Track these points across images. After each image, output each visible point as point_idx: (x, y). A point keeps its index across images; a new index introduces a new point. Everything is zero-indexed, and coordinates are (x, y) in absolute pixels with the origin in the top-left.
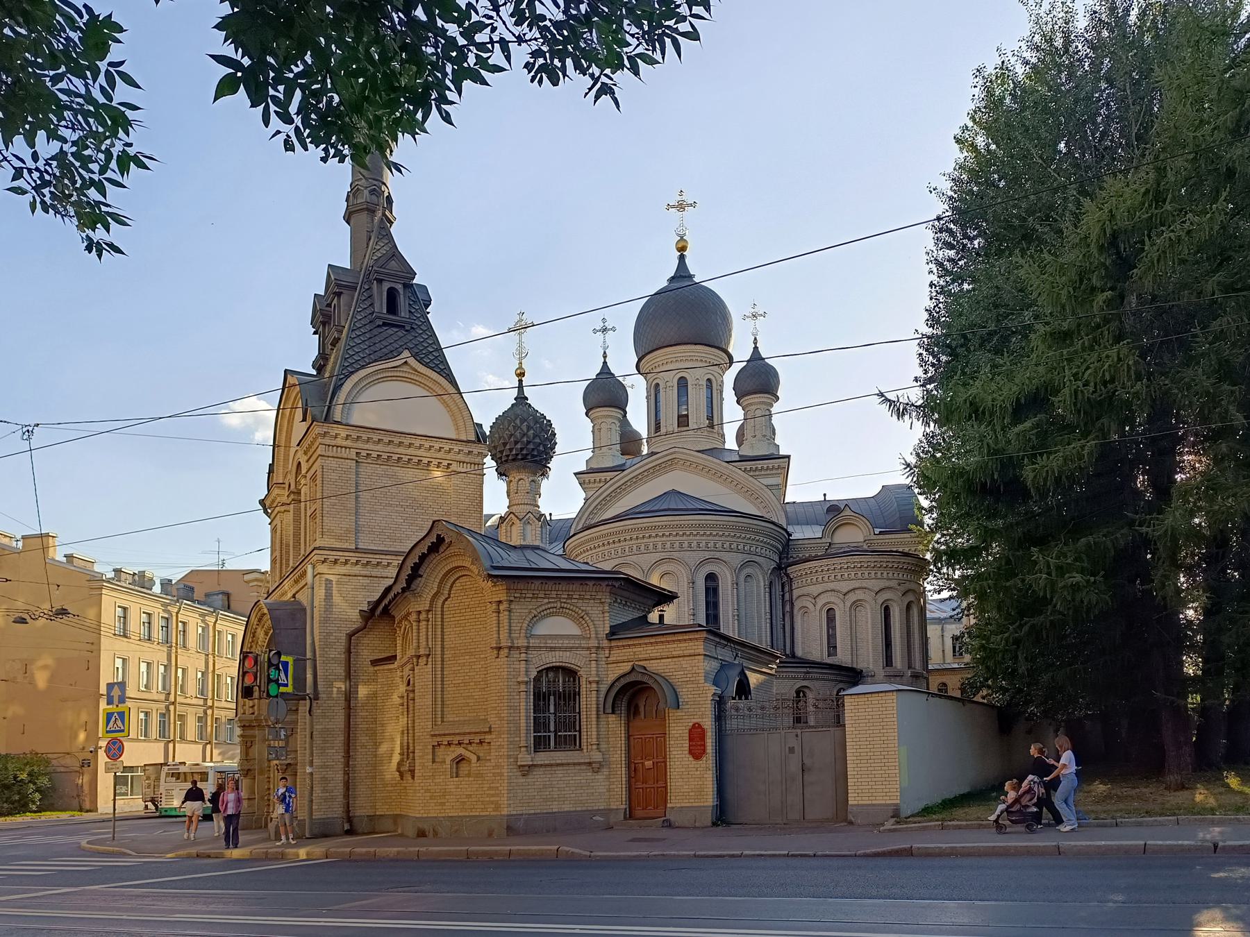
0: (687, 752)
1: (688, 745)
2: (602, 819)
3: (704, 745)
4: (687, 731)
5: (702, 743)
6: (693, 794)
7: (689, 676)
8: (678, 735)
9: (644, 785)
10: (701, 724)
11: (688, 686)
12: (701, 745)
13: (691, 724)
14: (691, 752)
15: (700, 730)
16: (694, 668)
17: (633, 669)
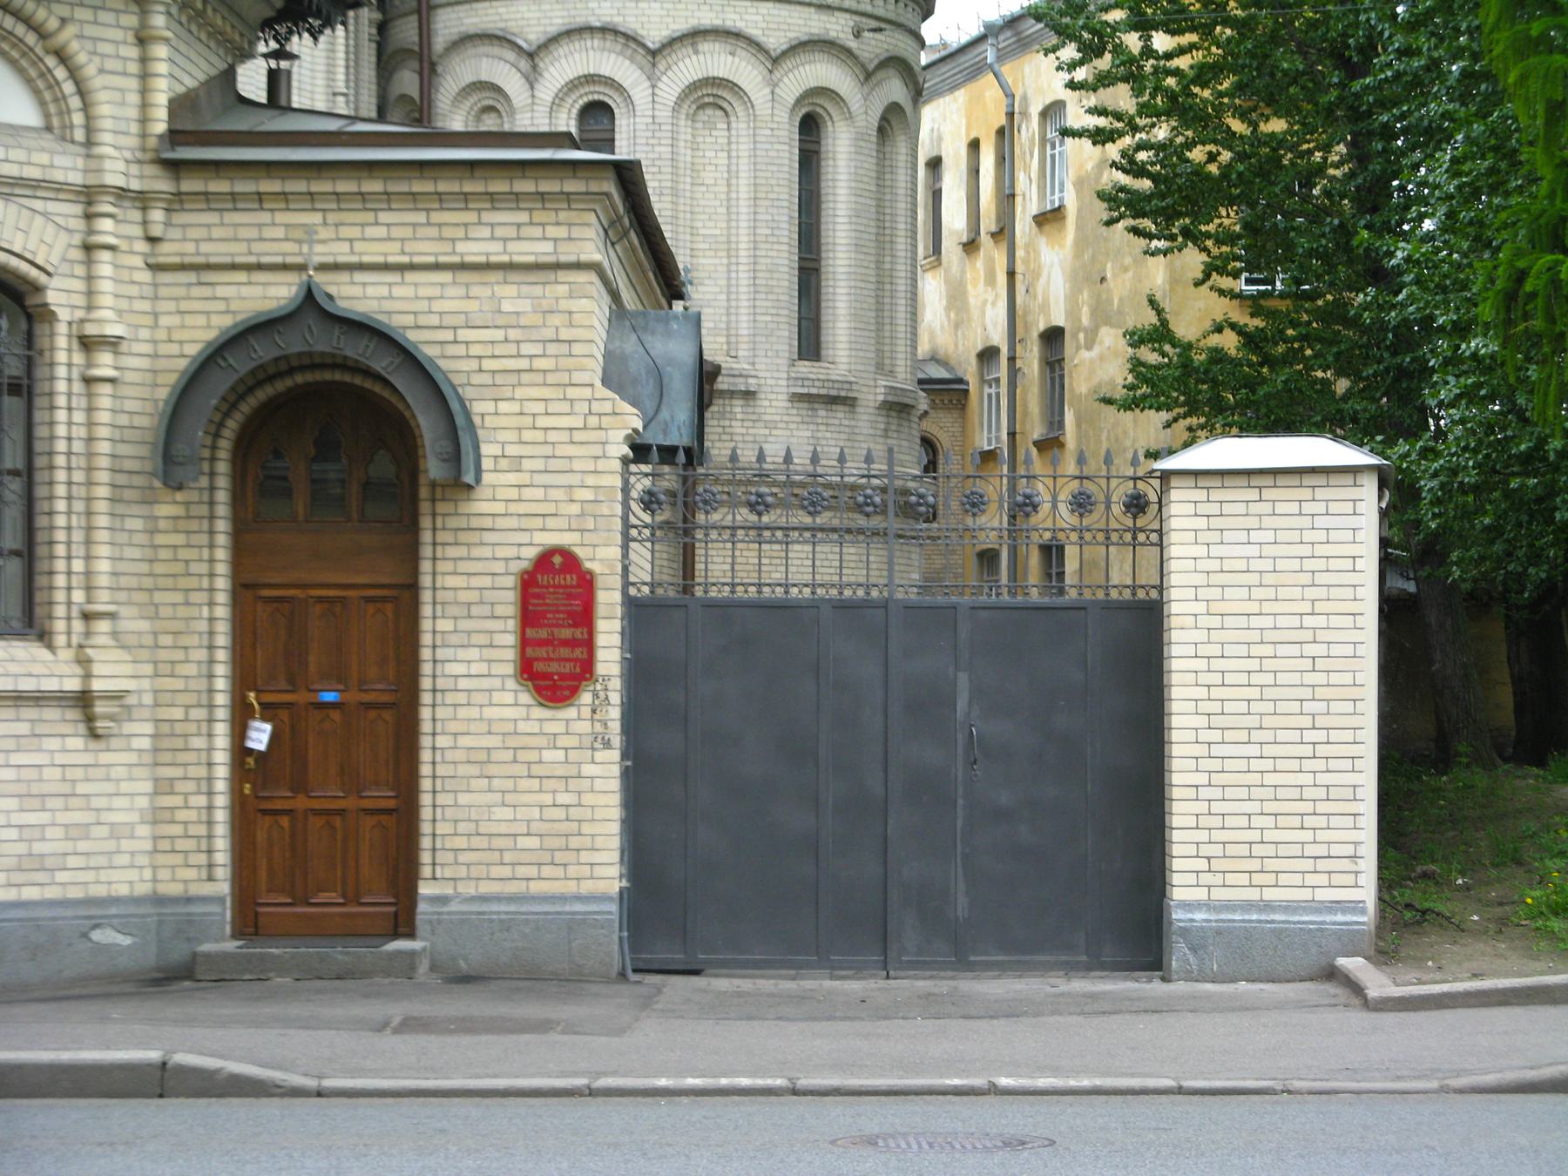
0: (509, 669)
1: (511, 639)
2: (125, 941)
3: (589, 644)
4: (510, 581)
5: (580, 633)
6: (533, 842)
7: (527, 349)
8: (473, 596)
9: (301, 803)
10: (580, 552)
11: (519, 392)
12: (571, 643)
13: (531, 553)
14: (528, 671)
15: (571, 579)
16: (556, 320)
17: (310, 300)
